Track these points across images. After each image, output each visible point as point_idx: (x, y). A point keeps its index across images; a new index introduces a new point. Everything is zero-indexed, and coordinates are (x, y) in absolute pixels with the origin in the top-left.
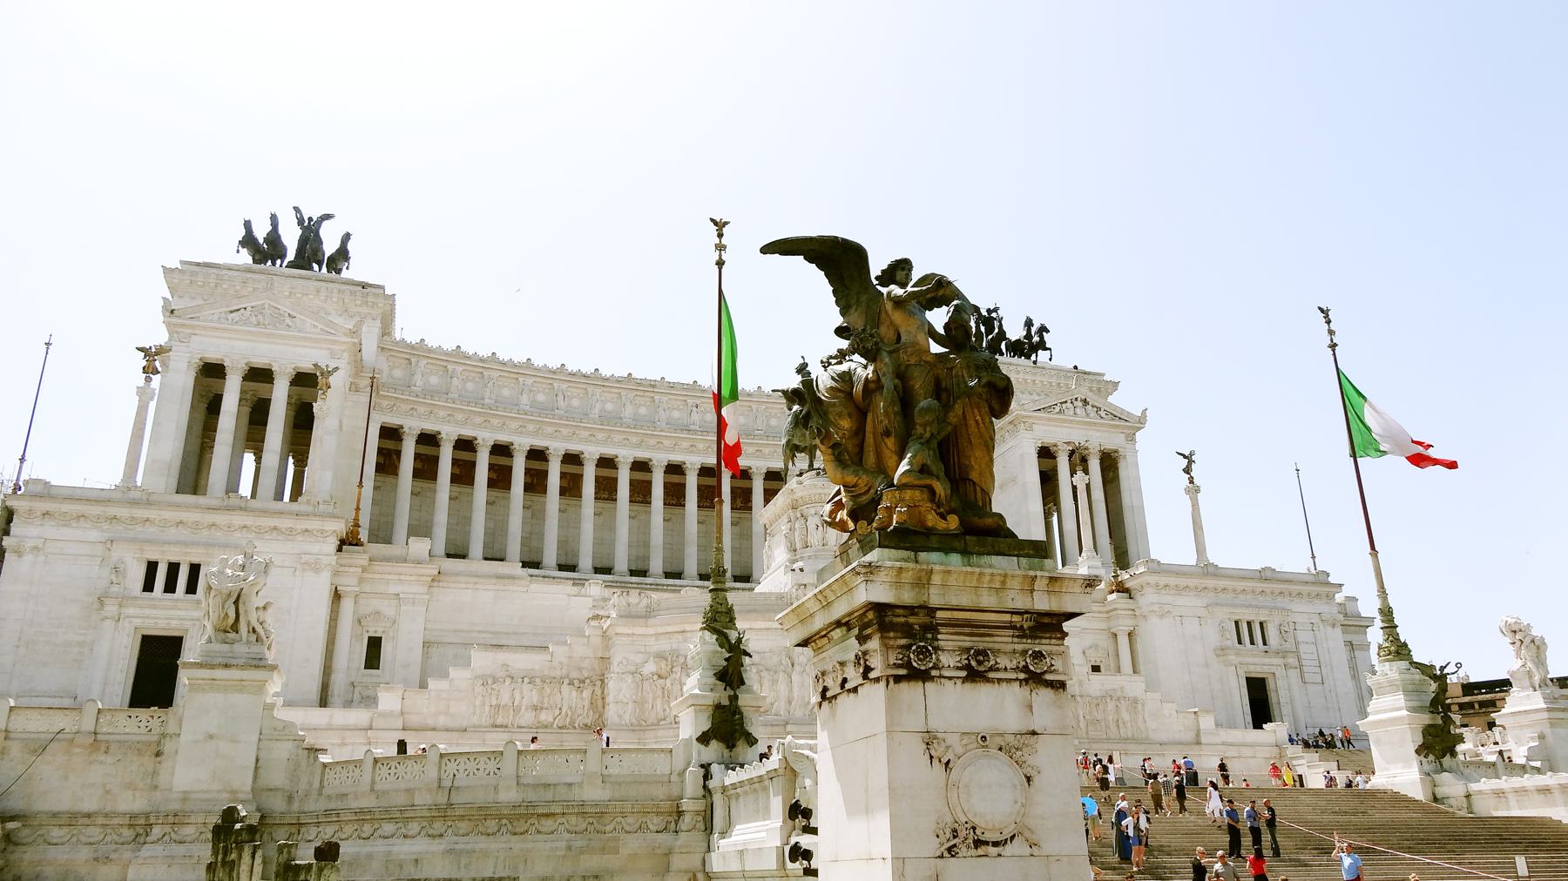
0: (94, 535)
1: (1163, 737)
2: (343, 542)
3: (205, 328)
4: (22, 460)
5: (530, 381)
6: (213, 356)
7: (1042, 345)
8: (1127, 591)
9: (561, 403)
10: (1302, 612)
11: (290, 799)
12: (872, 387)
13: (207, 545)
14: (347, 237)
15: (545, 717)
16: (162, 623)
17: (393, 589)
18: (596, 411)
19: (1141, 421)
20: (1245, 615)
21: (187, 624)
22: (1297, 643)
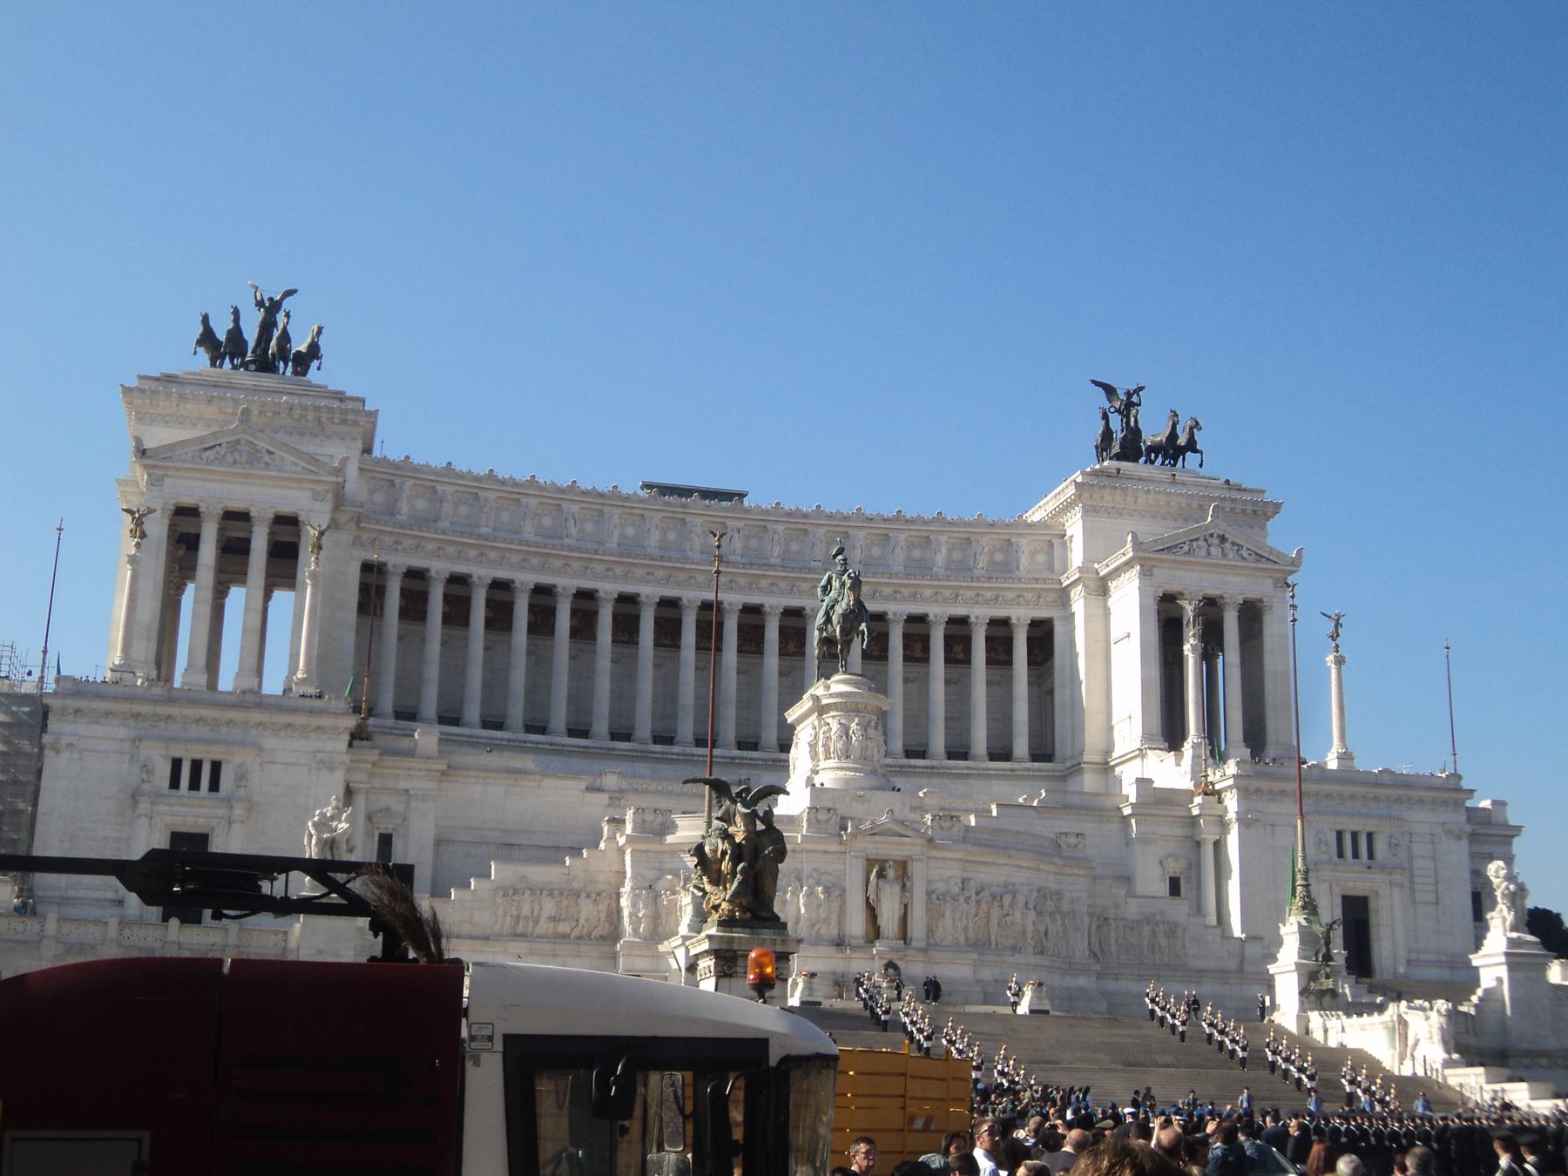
0: (122, 732)
1: (1201, 964)
2: (353, 736)
3: (178, 469)
4: (45, 652)
5: (533, 502)
6: (187, 500)
8: (1219, 793)
9: (573, 531)
10: (1421, 819)
12: (724, 853)
13: (225, 743)
14: (320, 330)
15: (563, 928)
16: (190, 820)
17: (403, 785)
18: (615, 538)
19: (1296, 563)
21: (213, 822)
22: (1411, 858)
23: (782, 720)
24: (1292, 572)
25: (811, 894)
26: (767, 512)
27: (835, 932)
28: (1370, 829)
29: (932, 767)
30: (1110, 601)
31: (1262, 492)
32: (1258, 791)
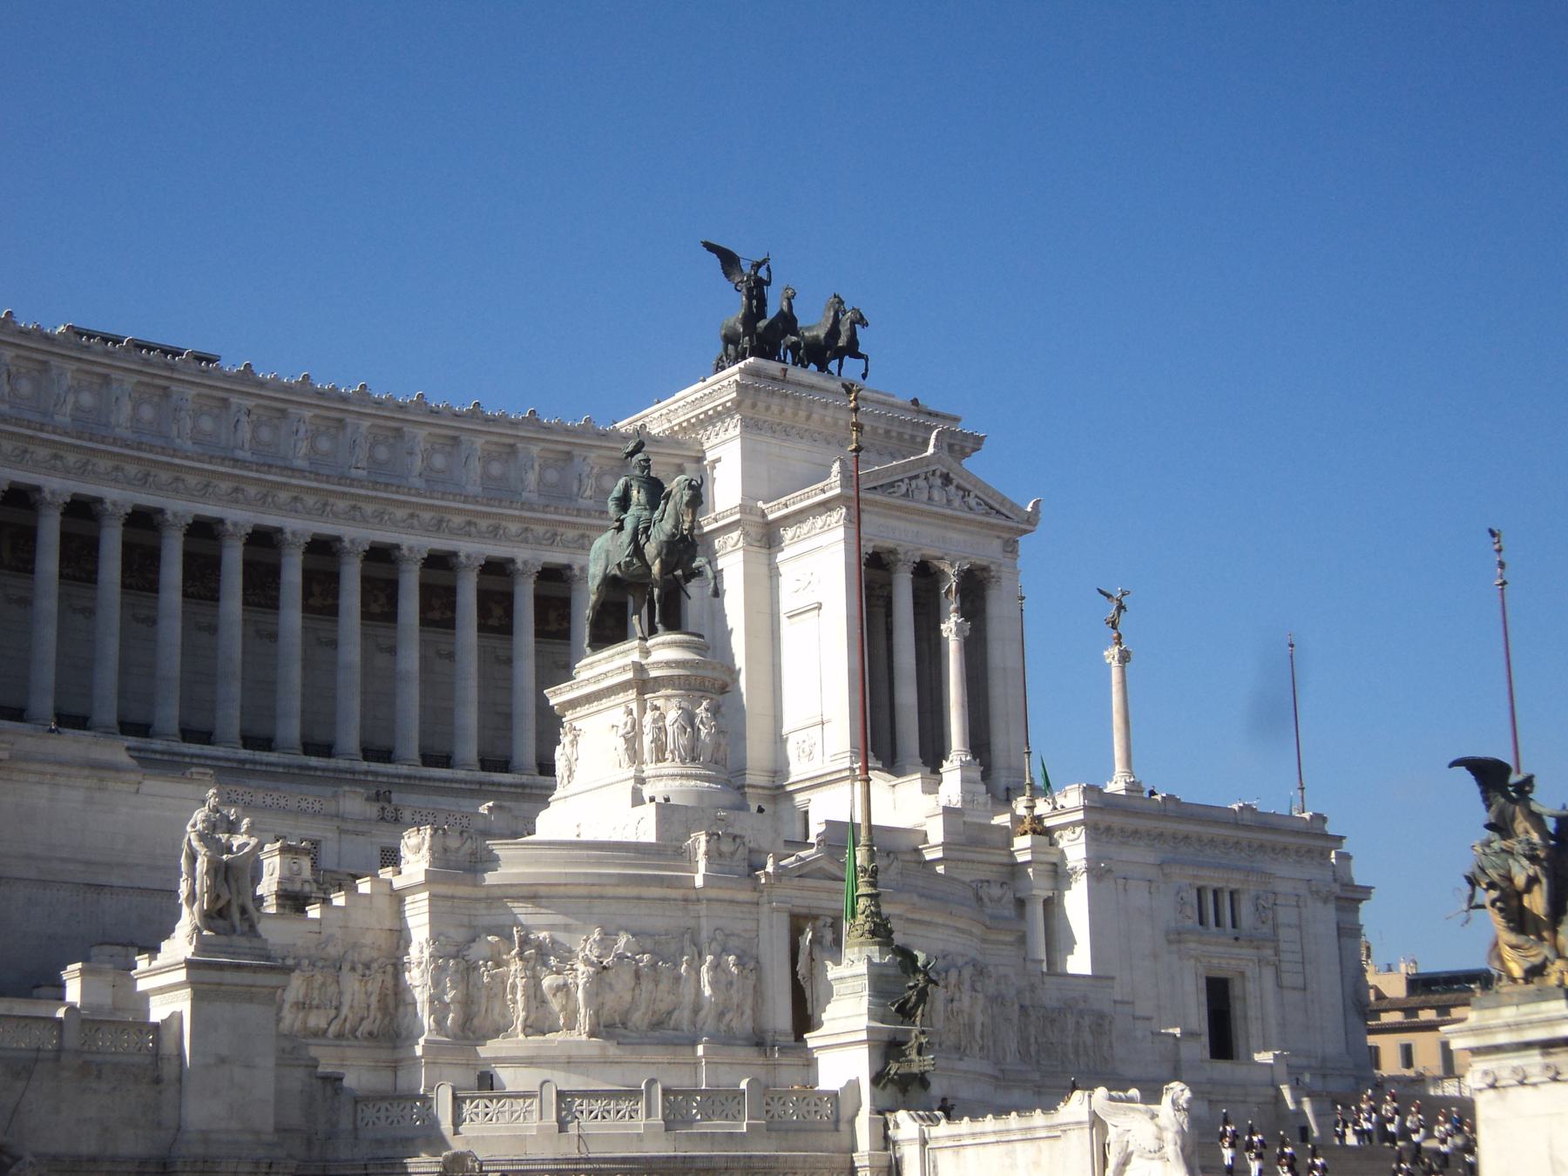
7: (852, 350)
8: (1048, 832)
10: (1287, 874)
11: (309, 1143)
15: (316, 1020)
18: (68, 408)
19: (1032, 520)
20: (1212, 879)
22: (1275, 927)
23: (542, 701)
24: (1025, 532)
25: (716, 967)
26: (288, 388)
27: (749, 1025)
28: (1233, 886)
29: (523, 786)
30: (780, 557)
31: (956, 420)
32: (1108, 829)
